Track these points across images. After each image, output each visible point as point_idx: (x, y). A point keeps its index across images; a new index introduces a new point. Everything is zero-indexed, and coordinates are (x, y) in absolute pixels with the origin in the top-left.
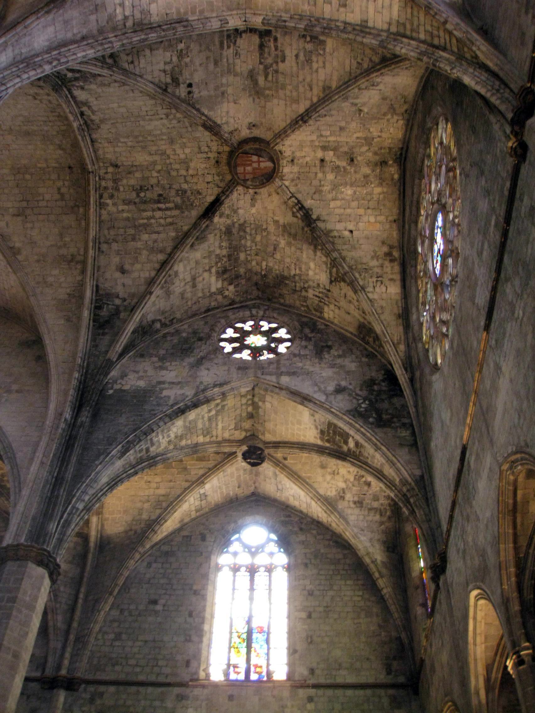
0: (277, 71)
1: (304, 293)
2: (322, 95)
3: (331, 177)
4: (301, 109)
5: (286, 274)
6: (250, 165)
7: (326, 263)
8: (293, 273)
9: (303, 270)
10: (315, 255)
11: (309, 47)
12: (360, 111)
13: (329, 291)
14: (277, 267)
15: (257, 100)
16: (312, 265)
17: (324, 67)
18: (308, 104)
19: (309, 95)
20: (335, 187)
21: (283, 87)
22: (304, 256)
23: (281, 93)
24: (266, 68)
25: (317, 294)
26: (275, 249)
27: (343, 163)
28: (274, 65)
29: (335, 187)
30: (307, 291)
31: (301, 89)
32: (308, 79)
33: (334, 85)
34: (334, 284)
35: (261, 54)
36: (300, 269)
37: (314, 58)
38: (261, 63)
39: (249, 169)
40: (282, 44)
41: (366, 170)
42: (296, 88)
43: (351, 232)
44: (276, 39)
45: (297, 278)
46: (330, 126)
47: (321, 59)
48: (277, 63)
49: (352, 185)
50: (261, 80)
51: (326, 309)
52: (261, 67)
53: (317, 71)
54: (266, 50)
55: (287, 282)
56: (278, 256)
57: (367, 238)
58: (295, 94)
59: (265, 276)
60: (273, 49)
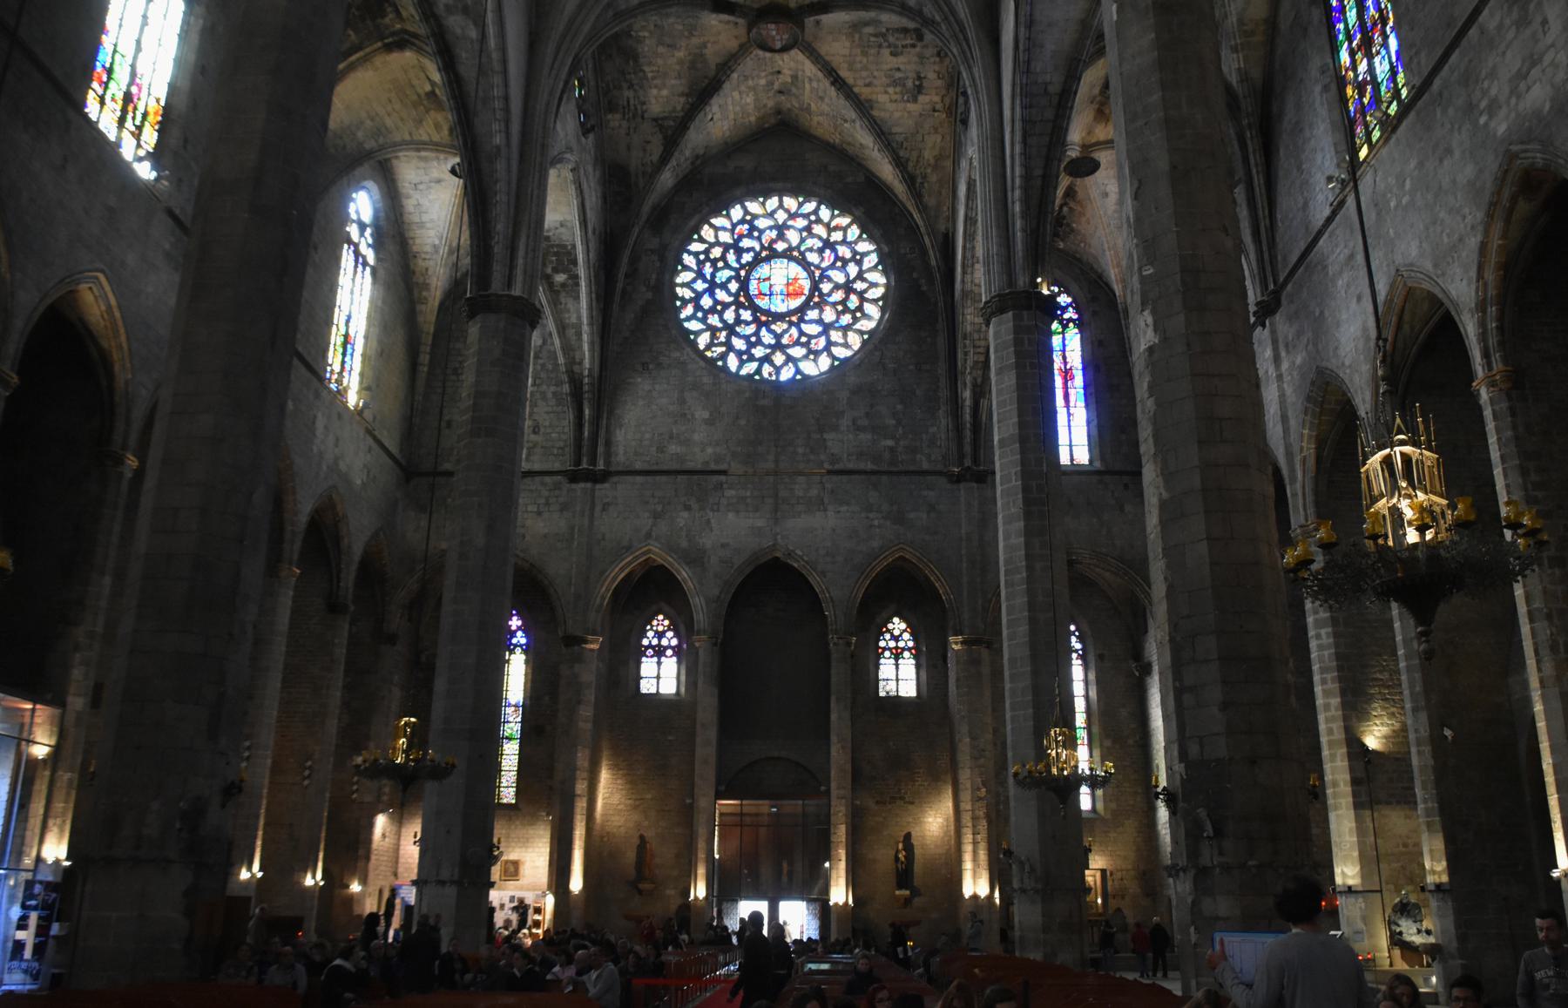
0: (880, 46)
1: (625, 85)
2: (862, 98)
3: (763, 82)
4: (844, 73)
5: (642, 60)
6: (778, 33)
7: (674, 110)
8: (646, 69)
9: (655, 82)
10: (679, 95)
11: (910, 84)
12: (846, 121)
13: (643, 117)
14: (646, 49)
15: (847, 26)
16: (665, 92)
17: (891, 101)
18: (850, 81)
19: (860, 82)
20: (754, 89)
21: (865, 54)
22: (673, 82)
23: (858, 51)
24: (883, 35)
25: (632, 102)
26: (669, 46)
27: (776, 87)
28: (886, 44)
29: (754, 89)
30: (629, 88)
31: (864, 74)
32: (875, 82)
33: (875, 113)
34: (654, 124)
35: (897, 30)
36: (654, 78)
37: (898, 89)
38: (888, 30)
39: (774, 33)
40: (909, 53)
41: (771, 104)
42: (865, 68)
43: (712, 119)
44: (913, 46)
45: (641, 74)
46: (825, 92)
47: (898, 97)
48: (889, 46)
49: (755, 100)
50: (869, 30)
51: (618, 116)
52: (884, 30)
53: (886, 92)
54: (902, 36)
55: (631, 63)
56: (661, 49)
57: (708, 133)
58: (859, 66)
59: (631, 36)
60: (904, 43)
